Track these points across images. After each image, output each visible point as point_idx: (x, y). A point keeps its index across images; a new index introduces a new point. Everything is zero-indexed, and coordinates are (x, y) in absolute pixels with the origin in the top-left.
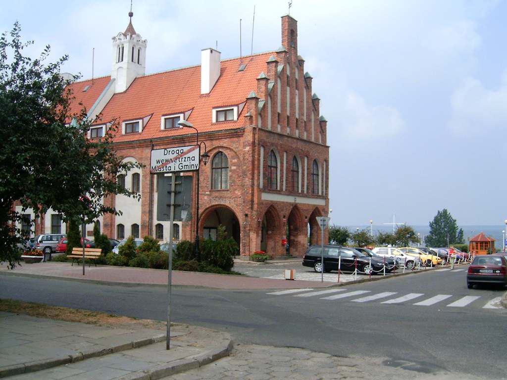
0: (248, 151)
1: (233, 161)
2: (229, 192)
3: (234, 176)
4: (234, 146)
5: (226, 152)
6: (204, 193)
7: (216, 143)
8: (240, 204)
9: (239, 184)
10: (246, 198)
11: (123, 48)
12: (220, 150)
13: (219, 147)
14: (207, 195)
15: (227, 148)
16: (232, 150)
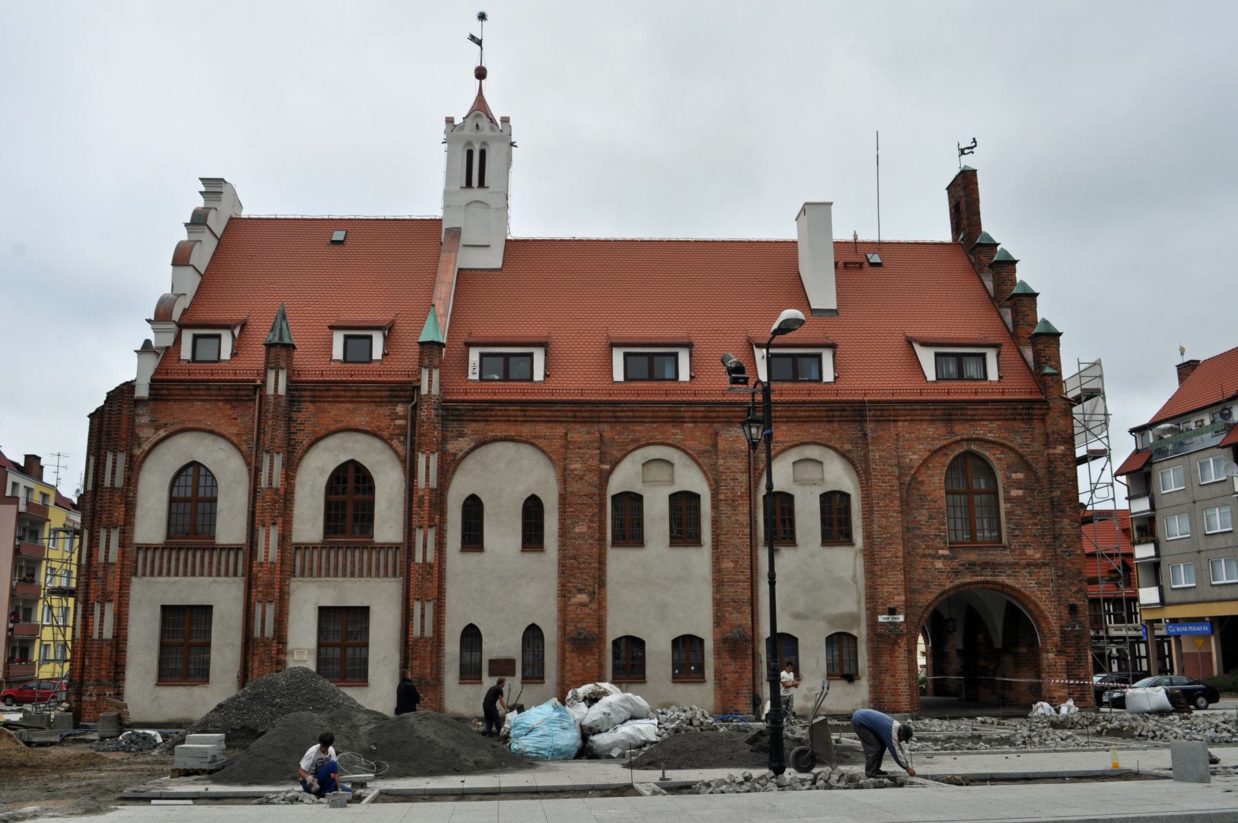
0: (1064, 456)
1: (1014, 476)
2: (1008, 552)
3: (1020, 513)
4: (1017, 442)
5: (991, 455)
6: (932, 552)
7: (963, 431)
8: (1045, 580)
9: (1034, 532)
10: (1069, 565)
11: (483, 153)
12: (974, 447)
13: (969, 440)
14: (943, 556)
15: (993, 443)
16: (1012, 449)
